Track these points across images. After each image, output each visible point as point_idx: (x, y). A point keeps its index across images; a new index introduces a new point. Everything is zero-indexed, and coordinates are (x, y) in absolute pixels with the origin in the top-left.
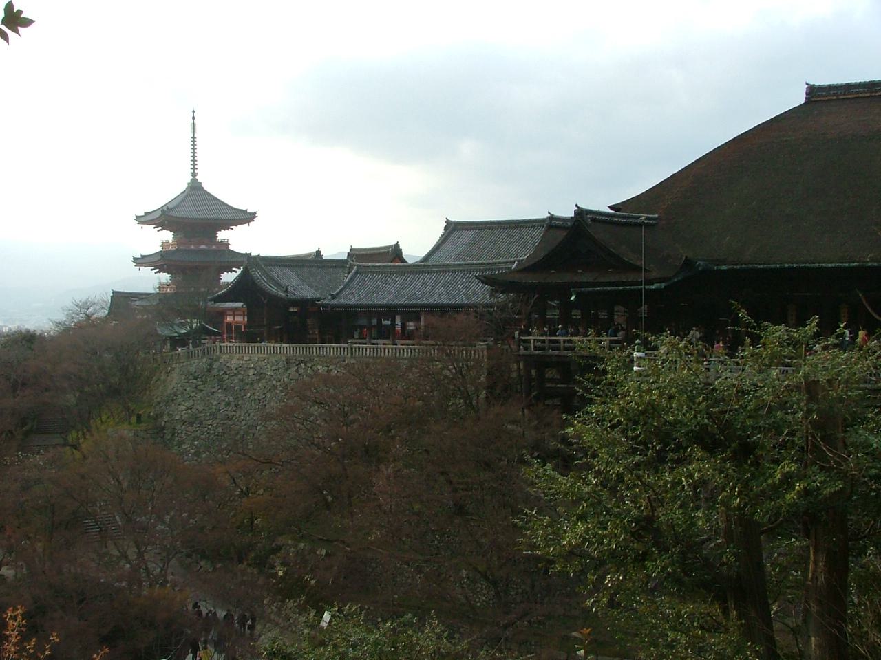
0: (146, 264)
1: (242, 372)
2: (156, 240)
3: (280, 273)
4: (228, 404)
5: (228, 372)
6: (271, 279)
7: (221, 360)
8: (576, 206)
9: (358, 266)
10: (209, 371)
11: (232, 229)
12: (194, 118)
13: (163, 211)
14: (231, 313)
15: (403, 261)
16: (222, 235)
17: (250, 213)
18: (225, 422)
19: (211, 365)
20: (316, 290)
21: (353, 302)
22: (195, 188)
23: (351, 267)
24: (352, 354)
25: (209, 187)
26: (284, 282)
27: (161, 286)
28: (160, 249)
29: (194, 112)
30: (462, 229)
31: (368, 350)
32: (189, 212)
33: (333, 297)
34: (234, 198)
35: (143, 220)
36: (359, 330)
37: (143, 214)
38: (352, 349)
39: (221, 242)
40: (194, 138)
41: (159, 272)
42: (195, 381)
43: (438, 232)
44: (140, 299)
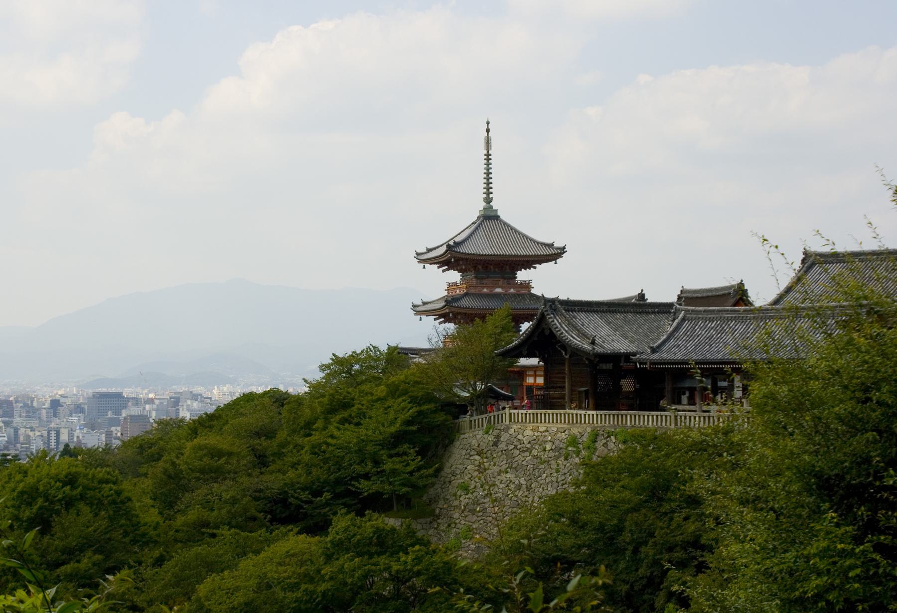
0: (428, 313)
1: (537, 447)
2: (440, 283)
3: (586, 321)
4: (519, 487)
5: (519, 447)
6: (575, 327)
7: (511, 431)
9: (687, 311)
10: (496, 444)
11: (535, 268)
12: (488, 131)
13: (449, 246)
14: (532, 373)
15: (748, 303)
16: (522, 275)
17: (557, 248)
18: (514, 510)
19: (498, 437)
20: (631, 342)
21: (679, 356)
22: (489, 217)
23: (677, 311)
24: (676, 424)
26: (590, 331)
28: (446, 293)
29: (488, 123)
30: (826, 262)
31: (697, 419)
32: (481, 247)
33: (654, 350)
36: (687, 394)
37: (425, 250)
38: (676, 417)
39: (521, 284)
40: (488, 155)
41: (445, 322)
42: (477, 457)
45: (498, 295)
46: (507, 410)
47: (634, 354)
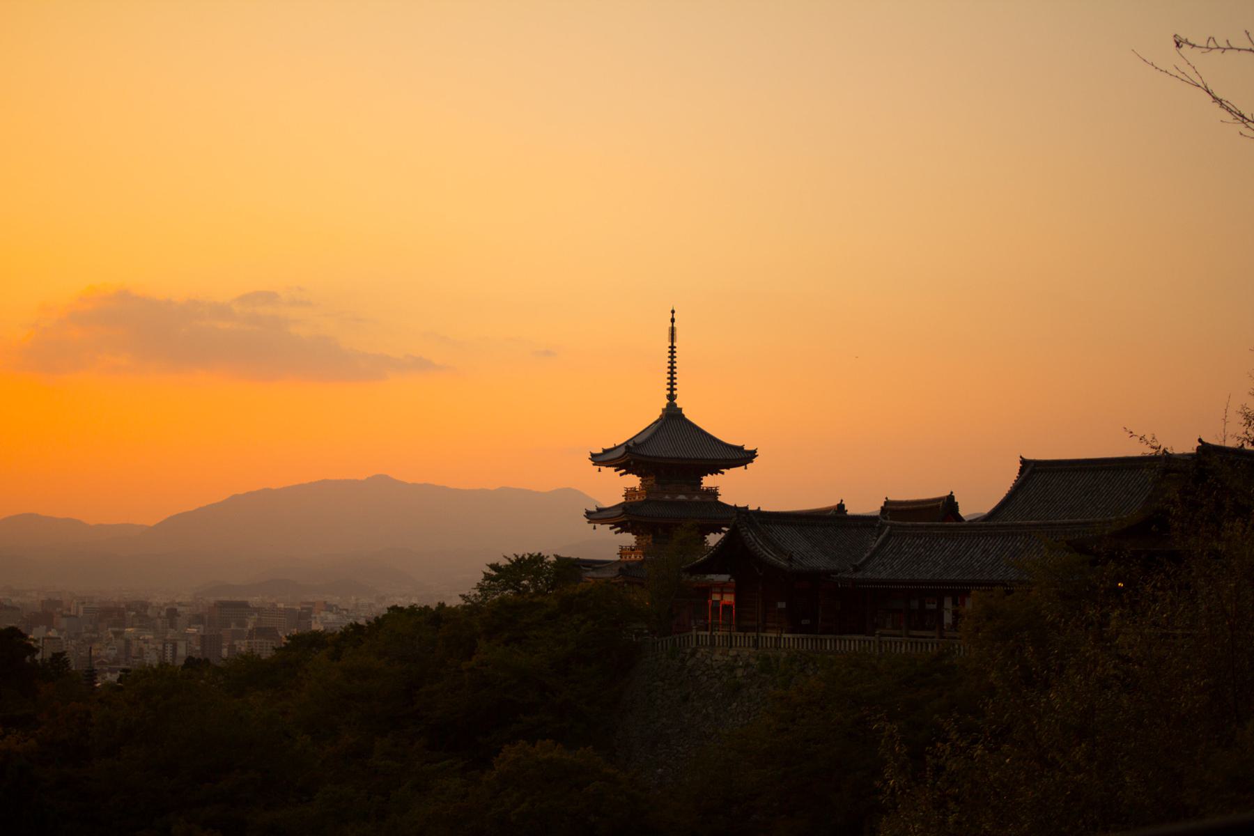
0: (603, 521)
2: (615, 487)
7: (699, 655)
8: (1200, 440)
9: (892, 526)
12: (673, 320)
15: (960, 519)
16: (708, 481)
21: (884, 576)
22: (672, 415)
23: (883, 526)
25: (689, 414)
27: (623, 551)
28: (623, 500)
29: (673, 312)
34: (726, 431)
35: (601, 459)
37: (600, 451)
40: (672, 347)
41: (621, 532)
43: (1008, 477)
44: (595, 569)
45: (682, 502)
46: (694, 632)
47: (835, 572)
